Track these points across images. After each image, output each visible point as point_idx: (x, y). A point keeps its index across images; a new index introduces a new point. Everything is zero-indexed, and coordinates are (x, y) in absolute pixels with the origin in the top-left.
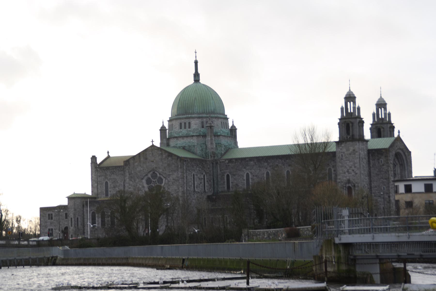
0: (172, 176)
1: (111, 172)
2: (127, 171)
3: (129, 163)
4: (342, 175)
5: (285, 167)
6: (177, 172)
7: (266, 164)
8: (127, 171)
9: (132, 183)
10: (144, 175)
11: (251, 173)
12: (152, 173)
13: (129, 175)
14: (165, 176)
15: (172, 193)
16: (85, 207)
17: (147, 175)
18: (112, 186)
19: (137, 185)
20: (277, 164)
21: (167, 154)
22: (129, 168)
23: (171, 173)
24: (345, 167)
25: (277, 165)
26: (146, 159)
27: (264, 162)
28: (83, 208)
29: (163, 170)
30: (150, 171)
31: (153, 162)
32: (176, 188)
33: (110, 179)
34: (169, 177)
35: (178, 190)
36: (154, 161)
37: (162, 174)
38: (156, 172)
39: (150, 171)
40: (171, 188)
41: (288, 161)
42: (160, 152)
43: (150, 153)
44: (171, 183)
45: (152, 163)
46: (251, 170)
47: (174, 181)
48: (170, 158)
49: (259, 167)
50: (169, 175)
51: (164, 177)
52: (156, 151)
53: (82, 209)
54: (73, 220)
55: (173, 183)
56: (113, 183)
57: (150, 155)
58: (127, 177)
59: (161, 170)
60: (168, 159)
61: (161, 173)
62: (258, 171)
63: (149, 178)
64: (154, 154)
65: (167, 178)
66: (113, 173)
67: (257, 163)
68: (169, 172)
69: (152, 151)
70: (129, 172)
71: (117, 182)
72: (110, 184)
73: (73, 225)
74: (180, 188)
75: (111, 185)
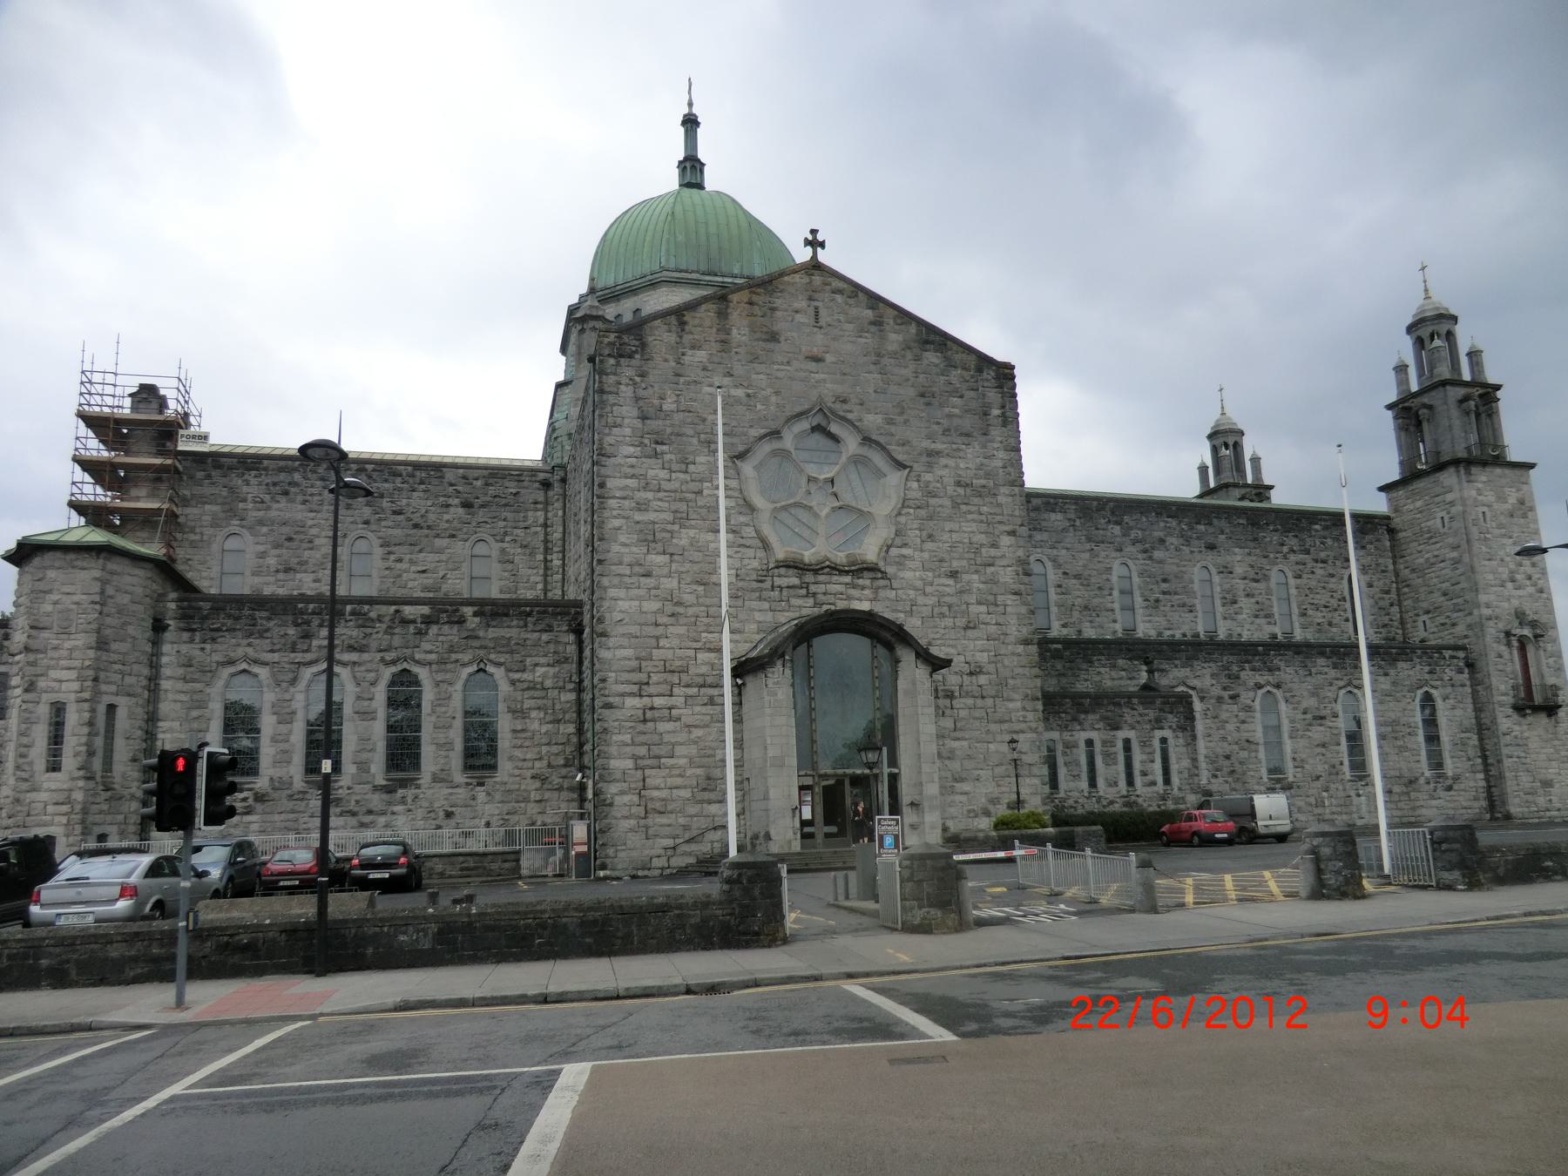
0: (951, 462)
1: (275, 484)
2: (626, 391)
3: (644, 345)
4: (1495, 589)
5: (1192, 552)
6: (984, 447)
7: (1117, 530)
8: (626, 391)
9: (663, 474)
10: (755, 432)
11: (1054, 560)
12: (805, 425)
13: (644, 418)
14: (900, 457)
15: (955, 564)
16: (168, 636)
17: (775, 434)
18: (272, 561)
19: (700, 492)
20: (1161, 534)
21: (913, 329)
22: (643, 375)
23: (939, 446)
24: (1502, 560)
25: (1162, 541)
26: (773, 337)
27: (1109, 521)
28: (156, 643)
29: (890, 422)
30: (800, 415)
31: (817, 359)
32: (981, 538)
33: (261, 522)
34: (930, 467)
35: (993, 552)
36: (829, 358)
37: (882, 440)
38: (834, 428)
39: (800, 415)
40: (946, 537)
41: (1202, 528)
42: (869, 314)
43: (801, 303)
44: (947, 502)
45: (812, 366)
46: (1053, 547)
47: (961, 491)
48: (932, 357)
49: (1089, 540)
50: (931, 454)
51: (901, 465)
52: (839, 298)
53: (148, 648)
54: (72, 718)
55: (956, 505)
56: (277, 546)
57: (799, 317)
58: (628, 431)
59: (872, 421)
60: (917, 359)
61: (874, 437)
62: (1087, 555)
63: (783, 454)
64: (823, 312)
65: (916, 466)
66: (286, 493)
67: (1078, 523)
68: (931, 437)
69: (811, 299)
70: (637, 399)
71: (311, 542)
72: (261, 548)
73: (69, 761)
74: (1006, 541)
75: (262, 555)
